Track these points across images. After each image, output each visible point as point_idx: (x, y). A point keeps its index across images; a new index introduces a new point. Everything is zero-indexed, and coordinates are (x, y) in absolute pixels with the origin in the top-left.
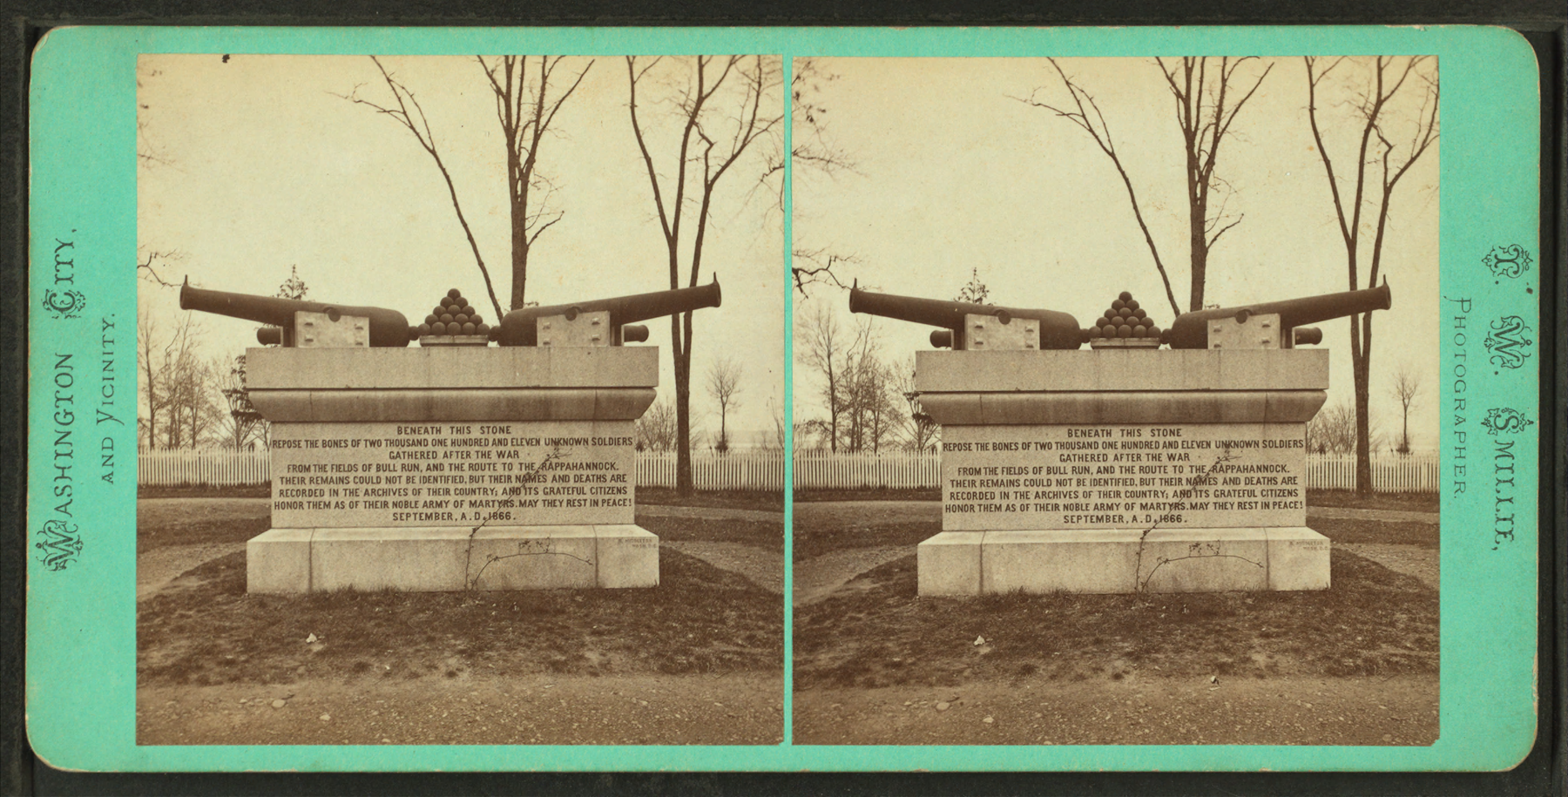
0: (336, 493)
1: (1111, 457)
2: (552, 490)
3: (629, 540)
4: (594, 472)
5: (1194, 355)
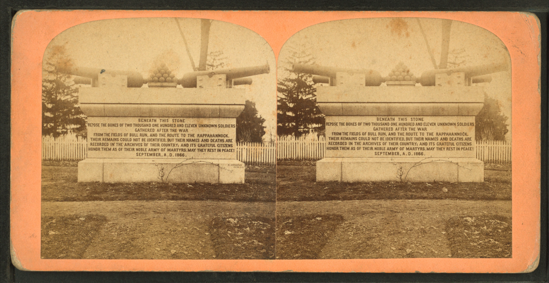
0: (351, 144)
1: (394, 129)
2: (440, 144)
3: (472, 163)
4: (458, 136)
5: (194, 88)
